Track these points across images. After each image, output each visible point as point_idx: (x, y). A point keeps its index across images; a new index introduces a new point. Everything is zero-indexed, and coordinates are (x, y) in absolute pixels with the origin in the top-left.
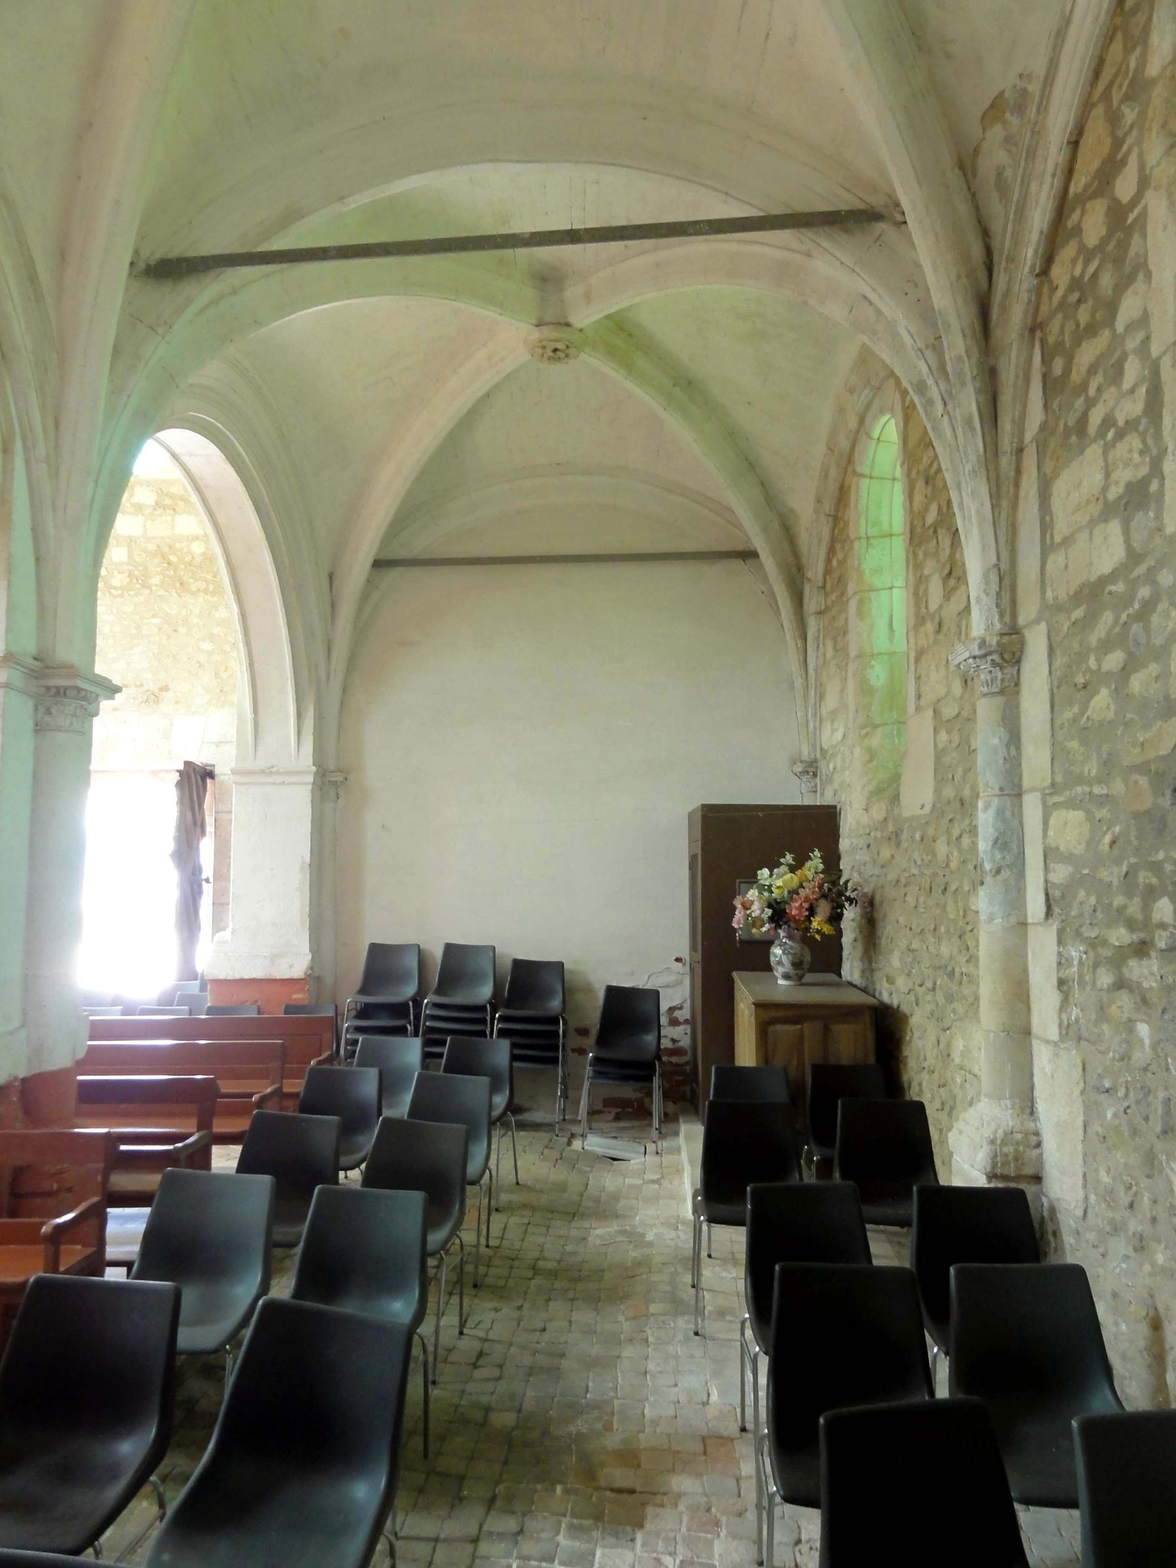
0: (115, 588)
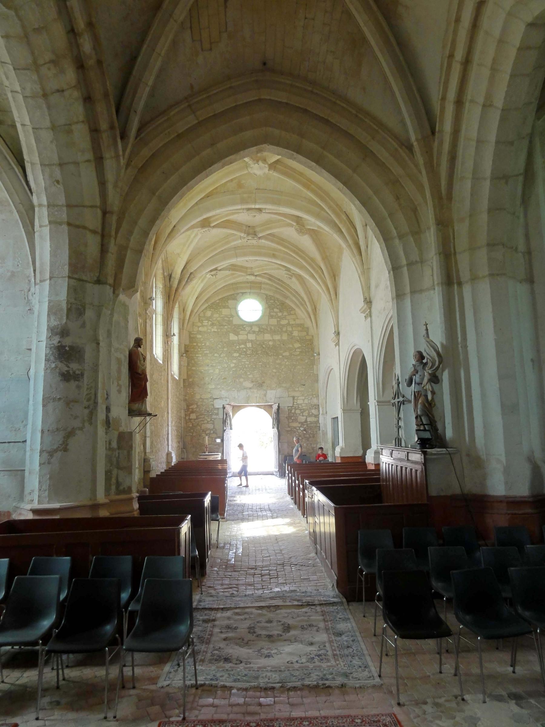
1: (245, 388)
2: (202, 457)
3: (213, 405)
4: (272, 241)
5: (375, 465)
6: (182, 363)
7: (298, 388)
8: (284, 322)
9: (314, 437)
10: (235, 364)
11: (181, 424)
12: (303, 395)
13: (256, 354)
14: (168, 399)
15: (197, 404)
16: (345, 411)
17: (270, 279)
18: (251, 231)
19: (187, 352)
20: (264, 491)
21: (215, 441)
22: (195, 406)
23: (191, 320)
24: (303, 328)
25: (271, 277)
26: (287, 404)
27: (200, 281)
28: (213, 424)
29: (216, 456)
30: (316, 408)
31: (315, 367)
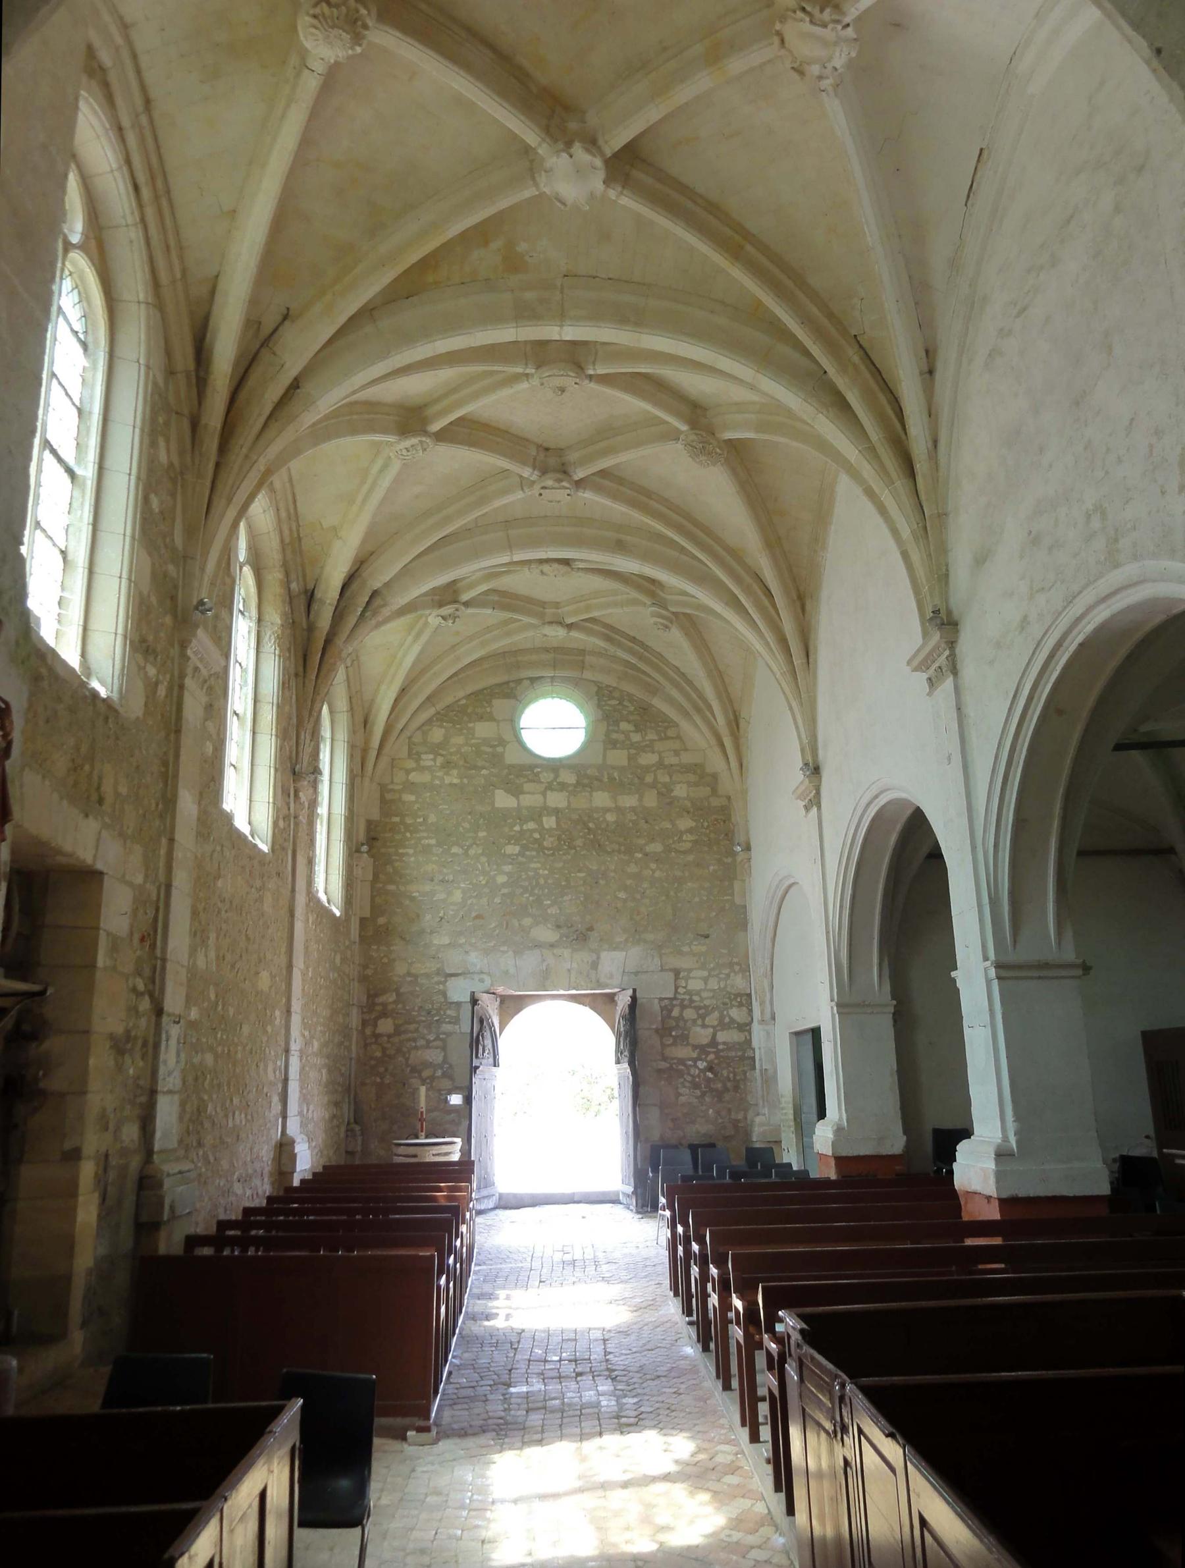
0: (548, 849)
1: (538, 945)
2: (401, 1150)
3: (444, 994)
4: (615, 496)
5: (1003, 1202)
6: (358, 872)
7: (690, 945)
9: (736, 1088)
10: (509, 874)
11: (349, 1049)
12: (703, 967)
13: (570, 848)
14: (290, 967)
15: (397, 991)
16: (845, 1007)
17: (608, 639)
18: (552, 461)
19: (372, 841)
20: (591, 1270)
21: (446, 1101)
22: (391, 998)
23: (386, 750)
24: (701, 774)
25: (611, 633)
26: (657, 989)
27: (410, 638)
28: (444, 1048)
29: (445, 1149)
30: (741, 1005)
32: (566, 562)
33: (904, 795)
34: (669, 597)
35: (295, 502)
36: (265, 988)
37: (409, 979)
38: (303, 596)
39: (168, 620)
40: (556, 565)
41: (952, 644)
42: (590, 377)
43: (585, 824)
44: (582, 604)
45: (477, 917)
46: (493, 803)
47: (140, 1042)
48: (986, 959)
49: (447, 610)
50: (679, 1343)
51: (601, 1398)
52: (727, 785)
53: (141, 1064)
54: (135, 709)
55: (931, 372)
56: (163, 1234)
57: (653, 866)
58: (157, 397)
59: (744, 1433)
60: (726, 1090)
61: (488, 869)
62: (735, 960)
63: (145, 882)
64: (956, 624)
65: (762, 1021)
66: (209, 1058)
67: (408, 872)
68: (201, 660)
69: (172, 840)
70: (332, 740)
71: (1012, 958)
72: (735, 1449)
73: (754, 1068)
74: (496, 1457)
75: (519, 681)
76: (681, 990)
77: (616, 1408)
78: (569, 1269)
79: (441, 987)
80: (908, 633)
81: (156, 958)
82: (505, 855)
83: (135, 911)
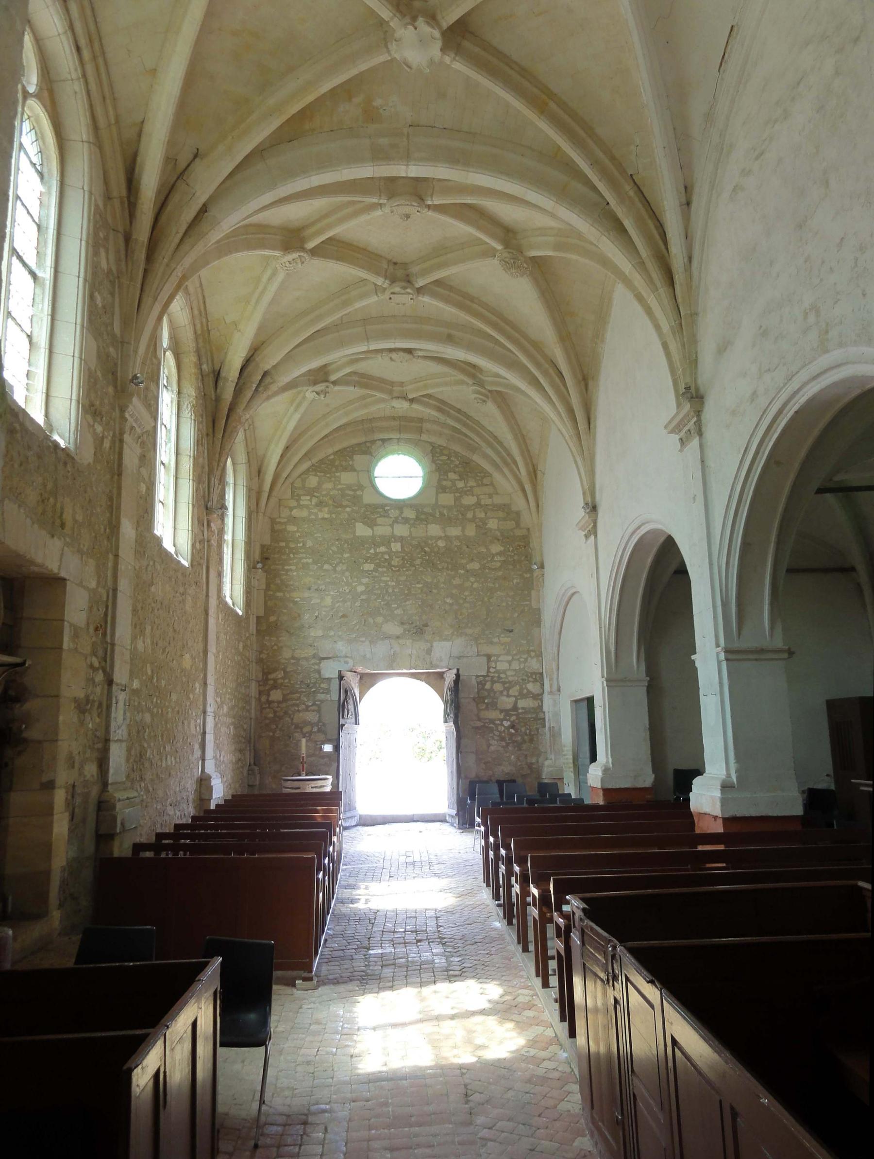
1: (388, 637)
2: (288, 784)
3: (319, 672)
4: (447, 300)
5: (725, 820)
6: (255, 583)
8: (469, 500)
9: (531, 740)
10: (367, 586)
11: (249, 711)
12: (508, 654)
14: (206, 652)
15: (284, 670)
16: (612, 682)
17: (439, 410)
18: (400, 273)
19: (265, 560)
21: (321, 749)
22: (280, 674)
23: (274, 493)
24: (507, 511)
25: (442, 406)
26: (475, 669)
27: (292, 409)
28: (319, 711)
29: (320, 783)
30: (535, 681)
31: (533, 593)
32: (409, 351)
33: (660, 527)
34: (487, 379)
35: (204, 302)
36: (188, 667)
37: (293, 661)
38: (212, 375)
39: (111, 390)
40: (401, 354)
41: (698, 413)
42: (429, 207)
43: (423, 550)
44: (422, 383)
45: (343, 616)
46: (355, 532)
47: (96, 704)
48: (718, 646)
49: (320, 387)
50: (490, 919)
51: (435, 957)
52: (527, 519)
53: (98, 720)
54: (87, 457)
55: (688, 204)
56: (116, 843)
57: (472, 579)
58: (98, 216)
59: (538, 982)
60: (524, 741)
61: (350, 581)
62: (531, 648)
63: (97, 587)
64: (702, 397)
65: (551, 693)
66: (148, 718)
67: (291, 583)
68: (136, 421)
69: (117, 556)
70: (235, 484)
71: (736, 645)
72: (531, 992)
73: (544, 726)
74: (360, 998)
75: (373, 442)
76: (492, 670)
77: (445, 965)
78: (411, 868)
79: (316, 667)
80: (666, 405)
81: (107, 643)
82: (363, 571)
83: (91, 608)
